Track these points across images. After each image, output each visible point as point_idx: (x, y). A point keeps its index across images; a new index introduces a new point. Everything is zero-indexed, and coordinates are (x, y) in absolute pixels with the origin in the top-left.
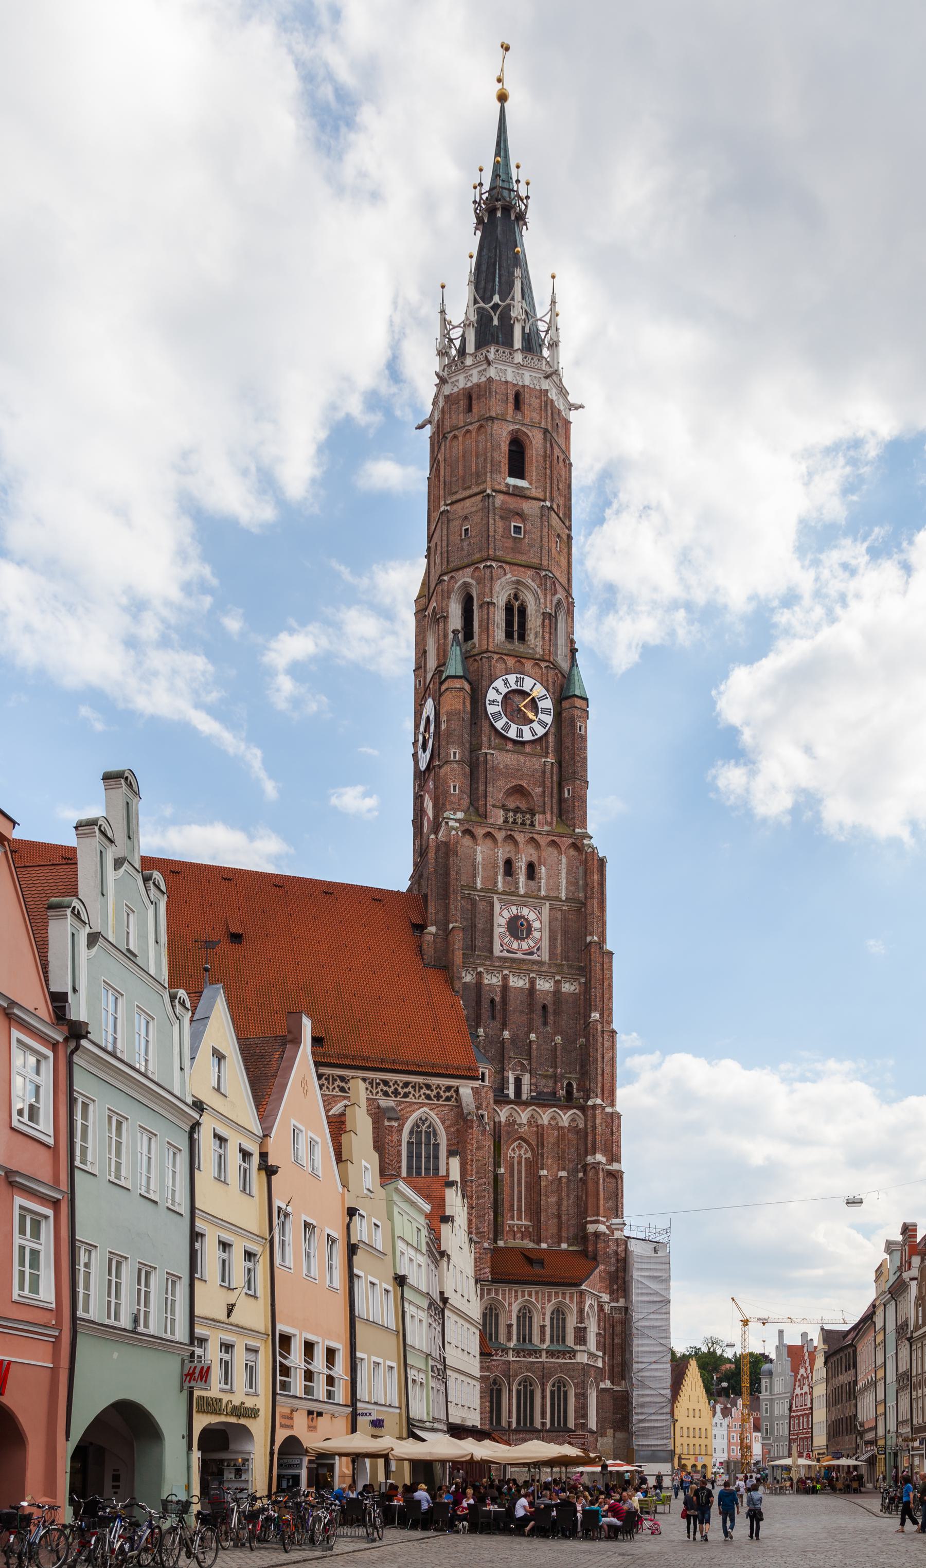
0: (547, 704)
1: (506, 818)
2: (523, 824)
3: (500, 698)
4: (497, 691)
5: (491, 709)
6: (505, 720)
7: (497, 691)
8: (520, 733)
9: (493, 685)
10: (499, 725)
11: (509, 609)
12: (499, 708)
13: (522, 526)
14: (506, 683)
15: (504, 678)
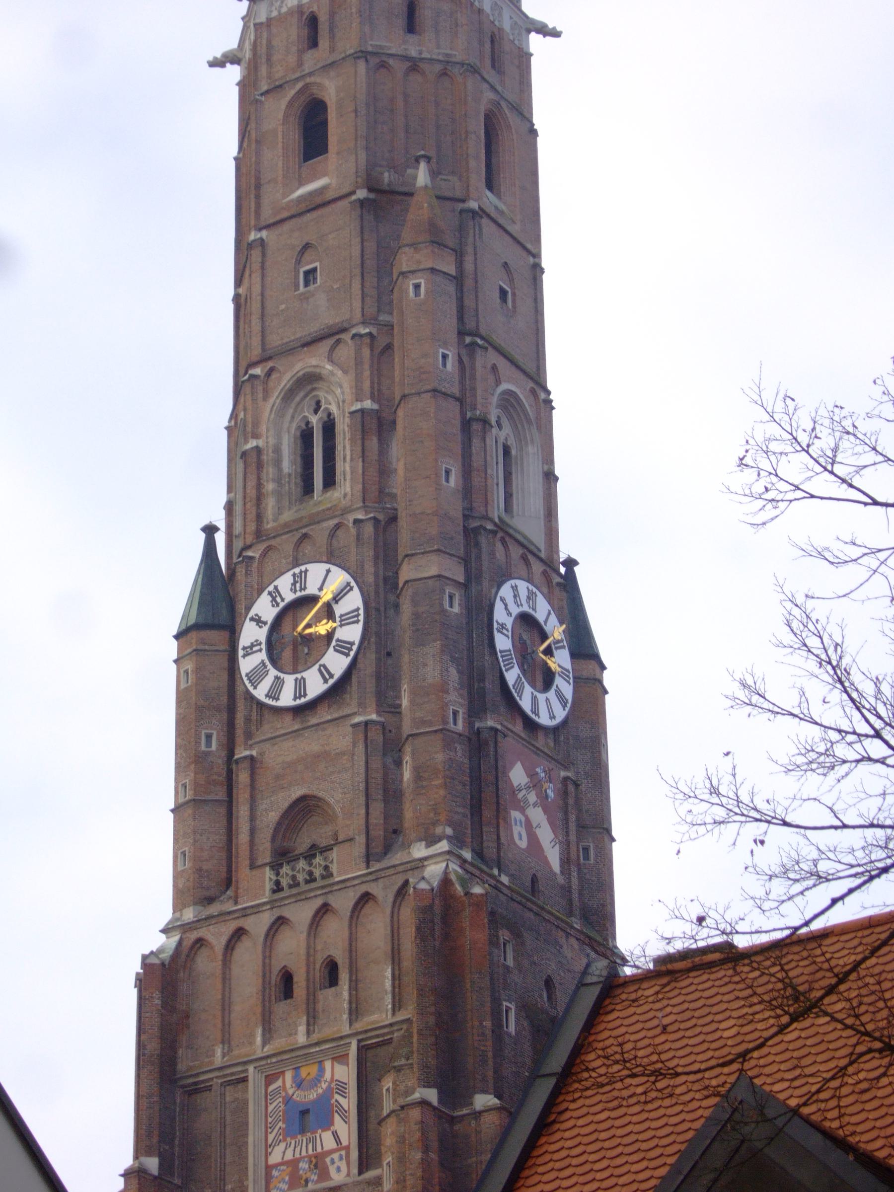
0: (354, 601)
1: (277, 883)
2: (311, 879)
3: (262, 634)
4: (258, 621)
5: (246, 665)
6: (273, 672)
7: (258, 621)
8: (300, 687)
9: (252, 613)
10: (260, 693)
11: (306, 436)
12: (263, 656)
13: (317, 264)
14: (275, 596)
15: (271, 588)
